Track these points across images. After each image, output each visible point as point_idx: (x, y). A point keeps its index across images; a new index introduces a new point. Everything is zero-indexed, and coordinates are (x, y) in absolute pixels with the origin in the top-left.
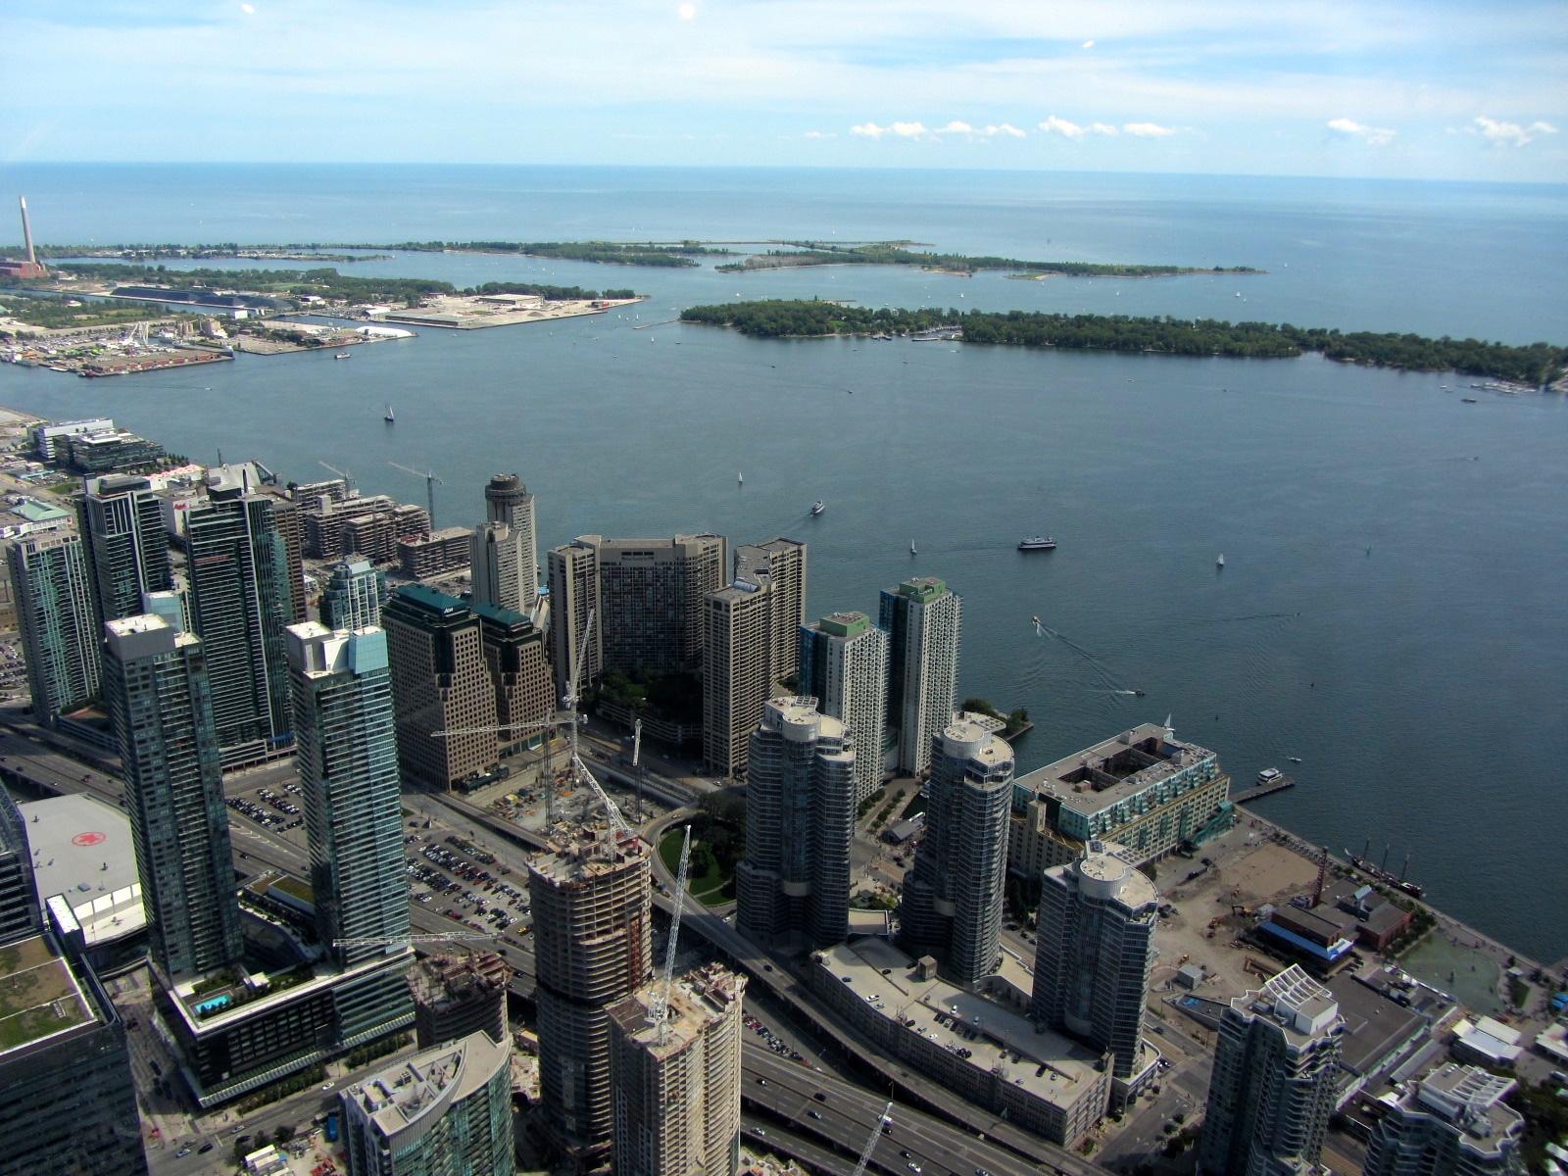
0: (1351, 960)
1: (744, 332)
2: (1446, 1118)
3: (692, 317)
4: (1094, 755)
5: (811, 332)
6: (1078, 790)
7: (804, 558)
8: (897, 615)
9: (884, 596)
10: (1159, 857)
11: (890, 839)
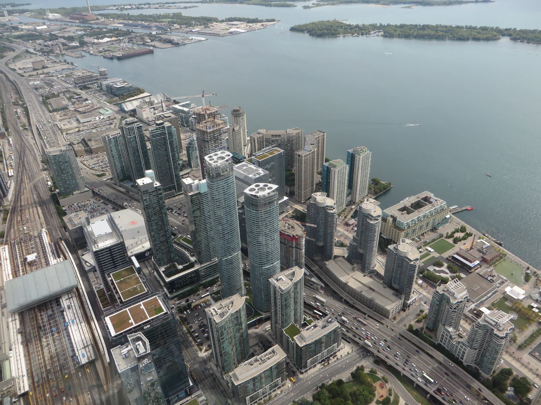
1: (310, 35)
2: (492, 325)
3: (293, 29)
4: (408, 201)
5: (333, 34)
7: (325, 137)
8: (351, 160)
9: (348, 152)
10: (426, 232)
11: (347, 224)
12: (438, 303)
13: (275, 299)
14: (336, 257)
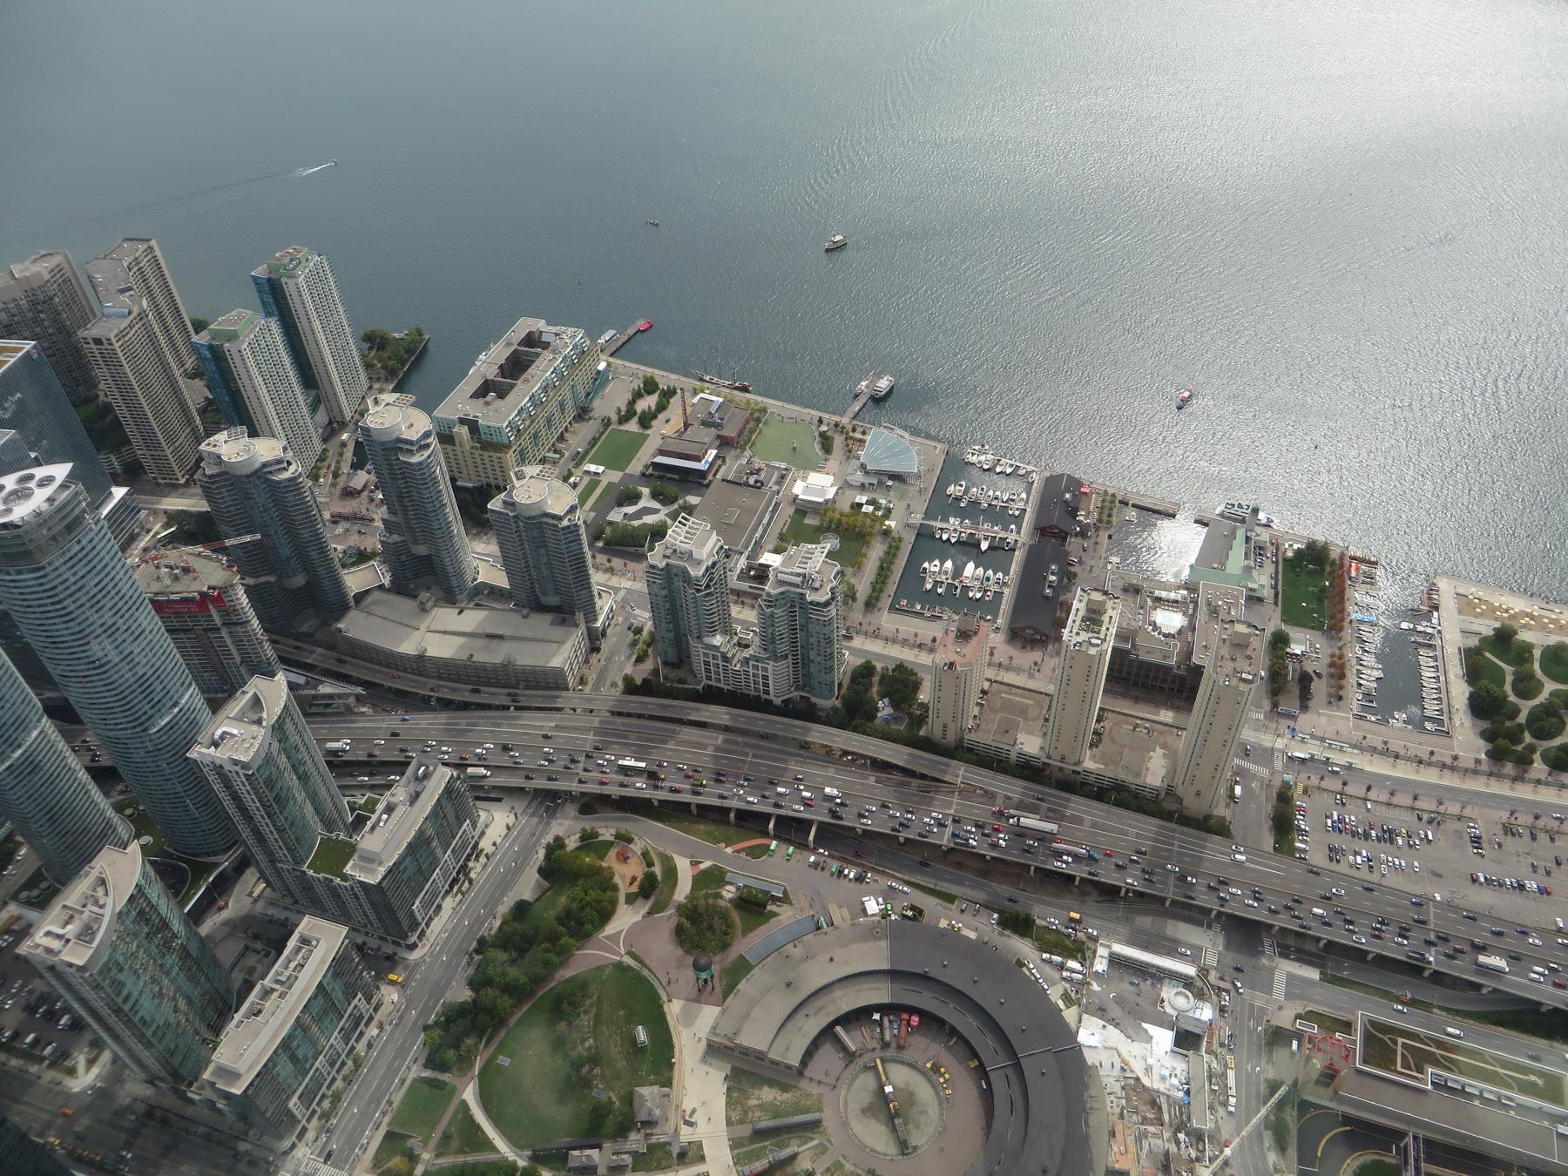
2: (797, 586)
4: (487, 363)
8: (275, 298)
9: (255, 278)
12: (664, 592)
13: (236, 798)
14: (360, 597)
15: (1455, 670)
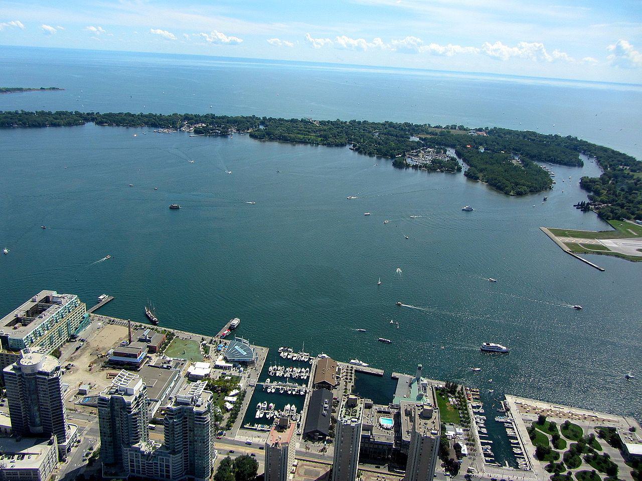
0: (148, 359)
2: (188, 404)
4: (21, 311)
6: (15, 328)
10: (62, 345)
15: (526, 437)
